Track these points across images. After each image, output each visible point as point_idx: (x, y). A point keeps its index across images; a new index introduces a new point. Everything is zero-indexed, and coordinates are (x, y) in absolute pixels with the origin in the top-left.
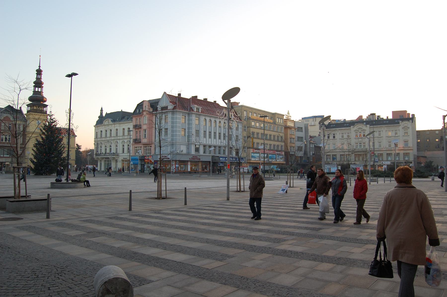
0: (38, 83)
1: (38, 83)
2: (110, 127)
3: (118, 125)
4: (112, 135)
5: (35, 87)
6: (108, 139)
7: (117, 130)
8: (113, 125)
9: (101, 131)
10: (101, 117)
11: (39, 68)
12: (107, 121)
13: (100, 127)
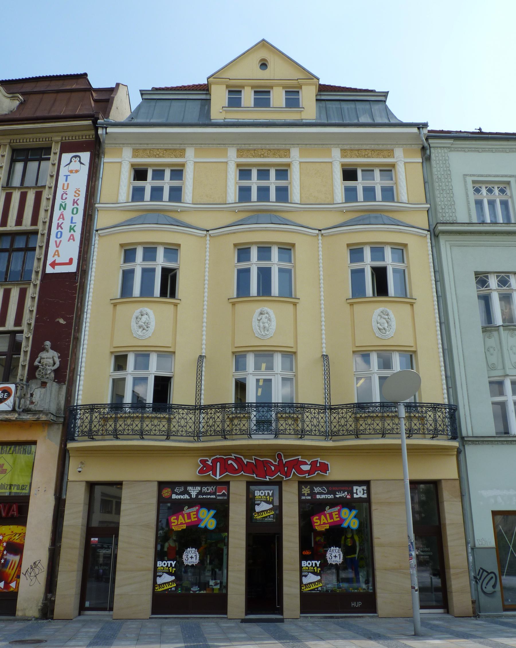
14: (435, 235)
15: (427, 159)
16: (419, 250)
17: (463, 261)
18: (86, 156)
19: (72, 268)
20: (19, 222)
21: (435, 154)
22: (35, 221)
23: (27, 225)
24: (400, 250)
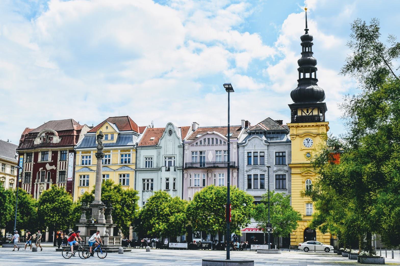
0: (307, 65)
1: (307, 65)
5: (300, 70)
11: (307, 33)
14: (136, 171)
15: (136, 152)
16: (132, 174)
17: (141, 176)
18: (73, 153)
19: (71, 180)
20: (63, 169)
21: (138, 151)
22: (65, 169)
23: (64, 170)
24: (128, 175)
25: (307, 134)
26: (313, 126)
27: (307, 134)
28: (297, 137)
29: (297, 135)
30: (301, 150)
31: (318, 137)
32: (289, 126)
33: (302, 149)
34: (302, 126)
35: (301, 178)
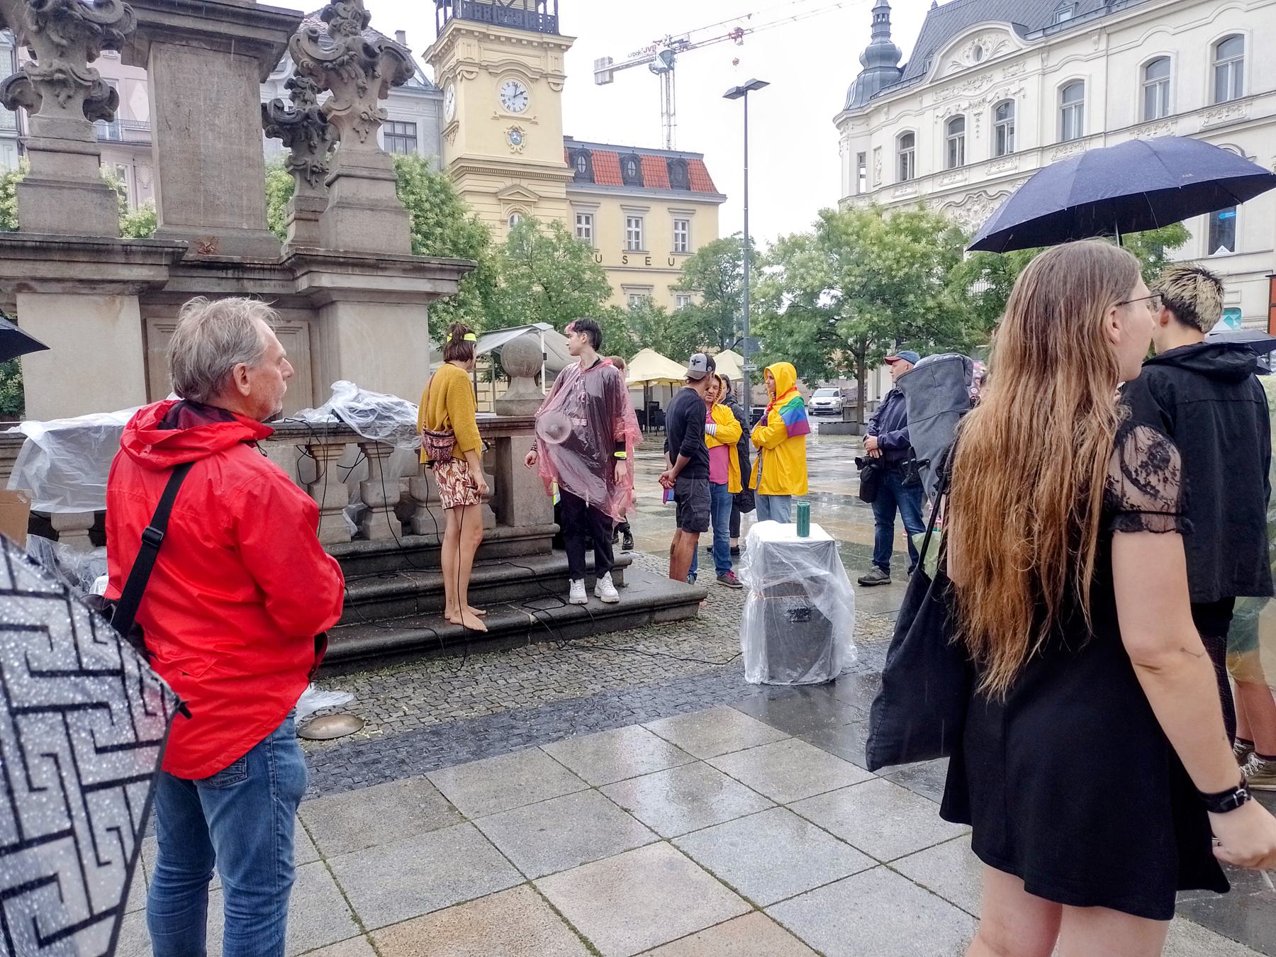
2: (997, 85)
3: (1085, 48)
4: (1024, 138)
6: (976, 176)
7: (1071, 89)
8: (1034, 64)
9: (907, 139)
10: (881, 57)
12: (956, 57)
13: (895, 112)
25: (516, 69)
26: (530, 43)
27: (516, 69)
28: (483, 73)
29: (480, 66)
30: (495, 118)
31: (543, 81)
32: (458, 30)
33: (499, 113)
34: (498, 37)
35: (497, 208)
